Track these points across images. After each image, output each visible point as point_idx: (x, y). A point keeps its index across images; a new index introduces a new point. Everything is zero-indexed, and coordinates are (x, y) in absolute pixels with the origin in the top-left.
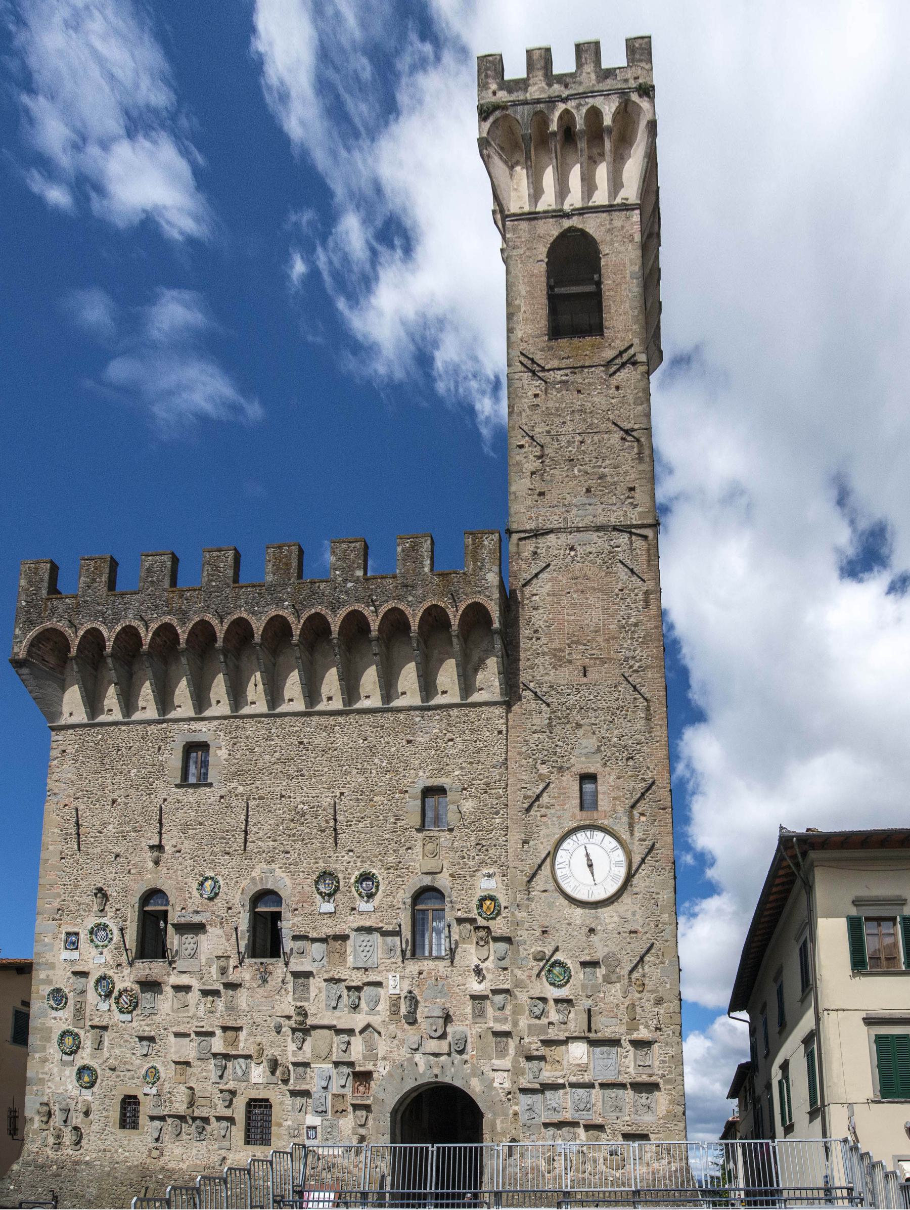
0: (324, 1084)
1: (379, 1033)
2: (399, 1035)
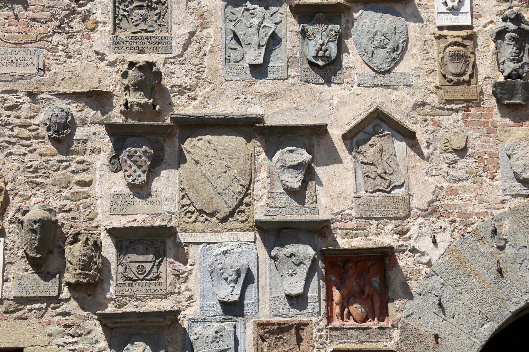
0: (230, 292)
1: (409, 136)
2: (478, 143)
